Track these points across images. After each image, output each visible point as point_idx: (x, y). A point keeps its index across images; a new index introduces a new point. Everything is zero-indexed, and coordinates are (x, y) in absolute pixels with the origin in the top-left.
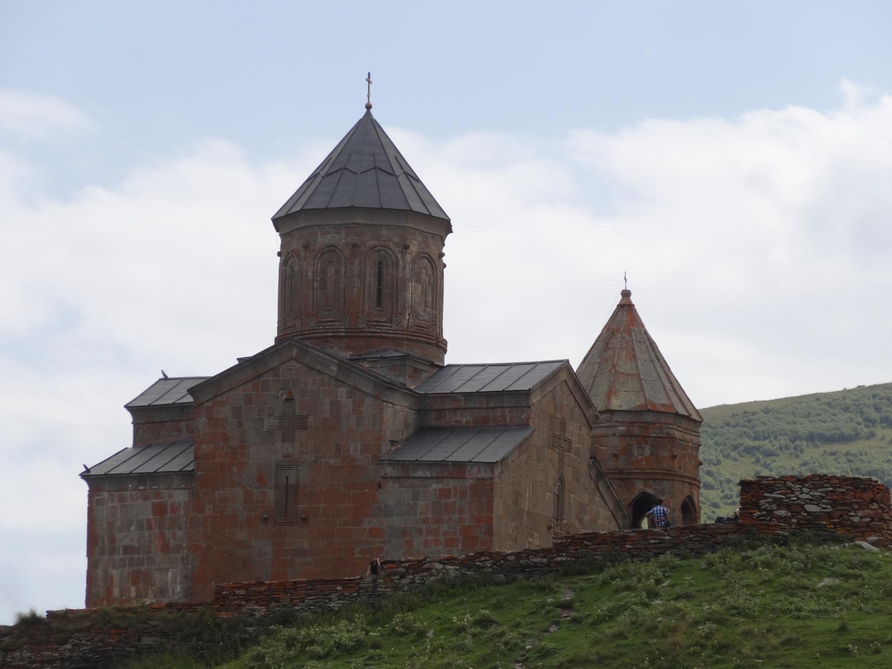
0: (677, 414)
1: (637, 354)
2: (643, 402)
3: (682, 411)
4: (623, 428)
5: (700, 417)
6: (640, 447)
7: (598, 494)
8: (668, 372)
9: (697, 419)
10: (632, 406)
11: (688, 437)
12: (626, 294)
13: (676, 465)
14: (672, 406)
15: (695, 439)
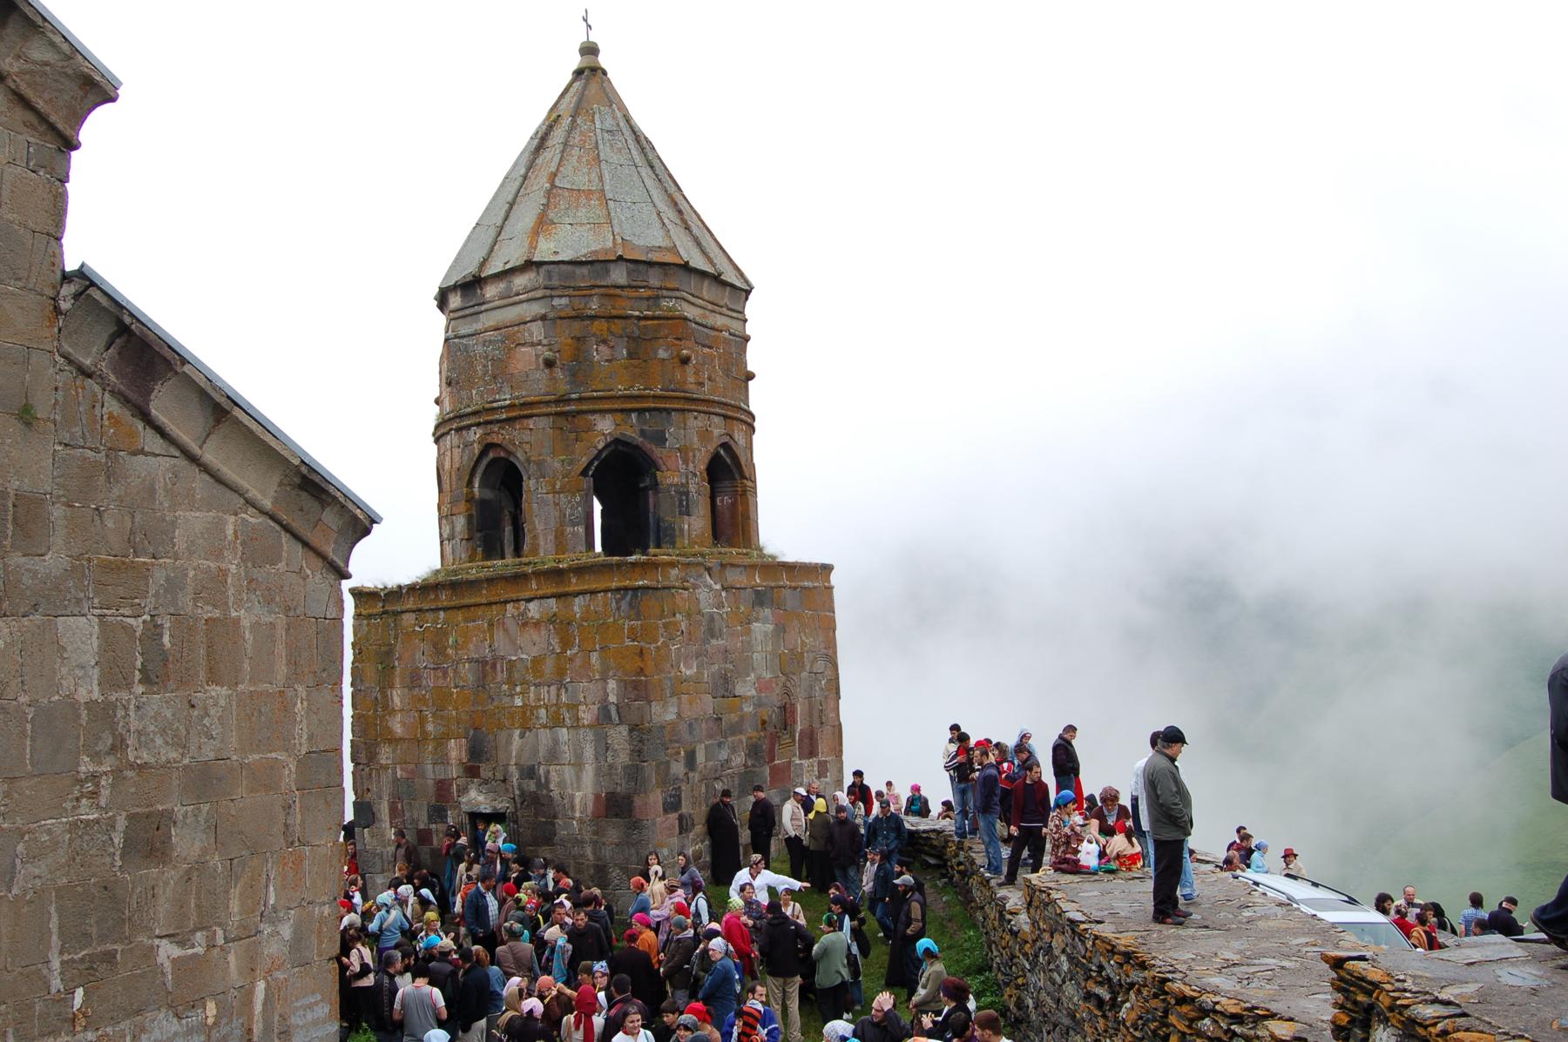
0: (686, 267)
1: (605, 151)
2: (610, 244)
3: (698, 262)
4: (564, 301)
5: (747, 281)
6: (605, 342)
7: (153, 442)
8: (672, 189)
9: (738, 283)
10: (584, 251)
11: (720, 321)
12: (590, 50)
13: (691, 379)
14: (673, 249)
15: (735, 325)
